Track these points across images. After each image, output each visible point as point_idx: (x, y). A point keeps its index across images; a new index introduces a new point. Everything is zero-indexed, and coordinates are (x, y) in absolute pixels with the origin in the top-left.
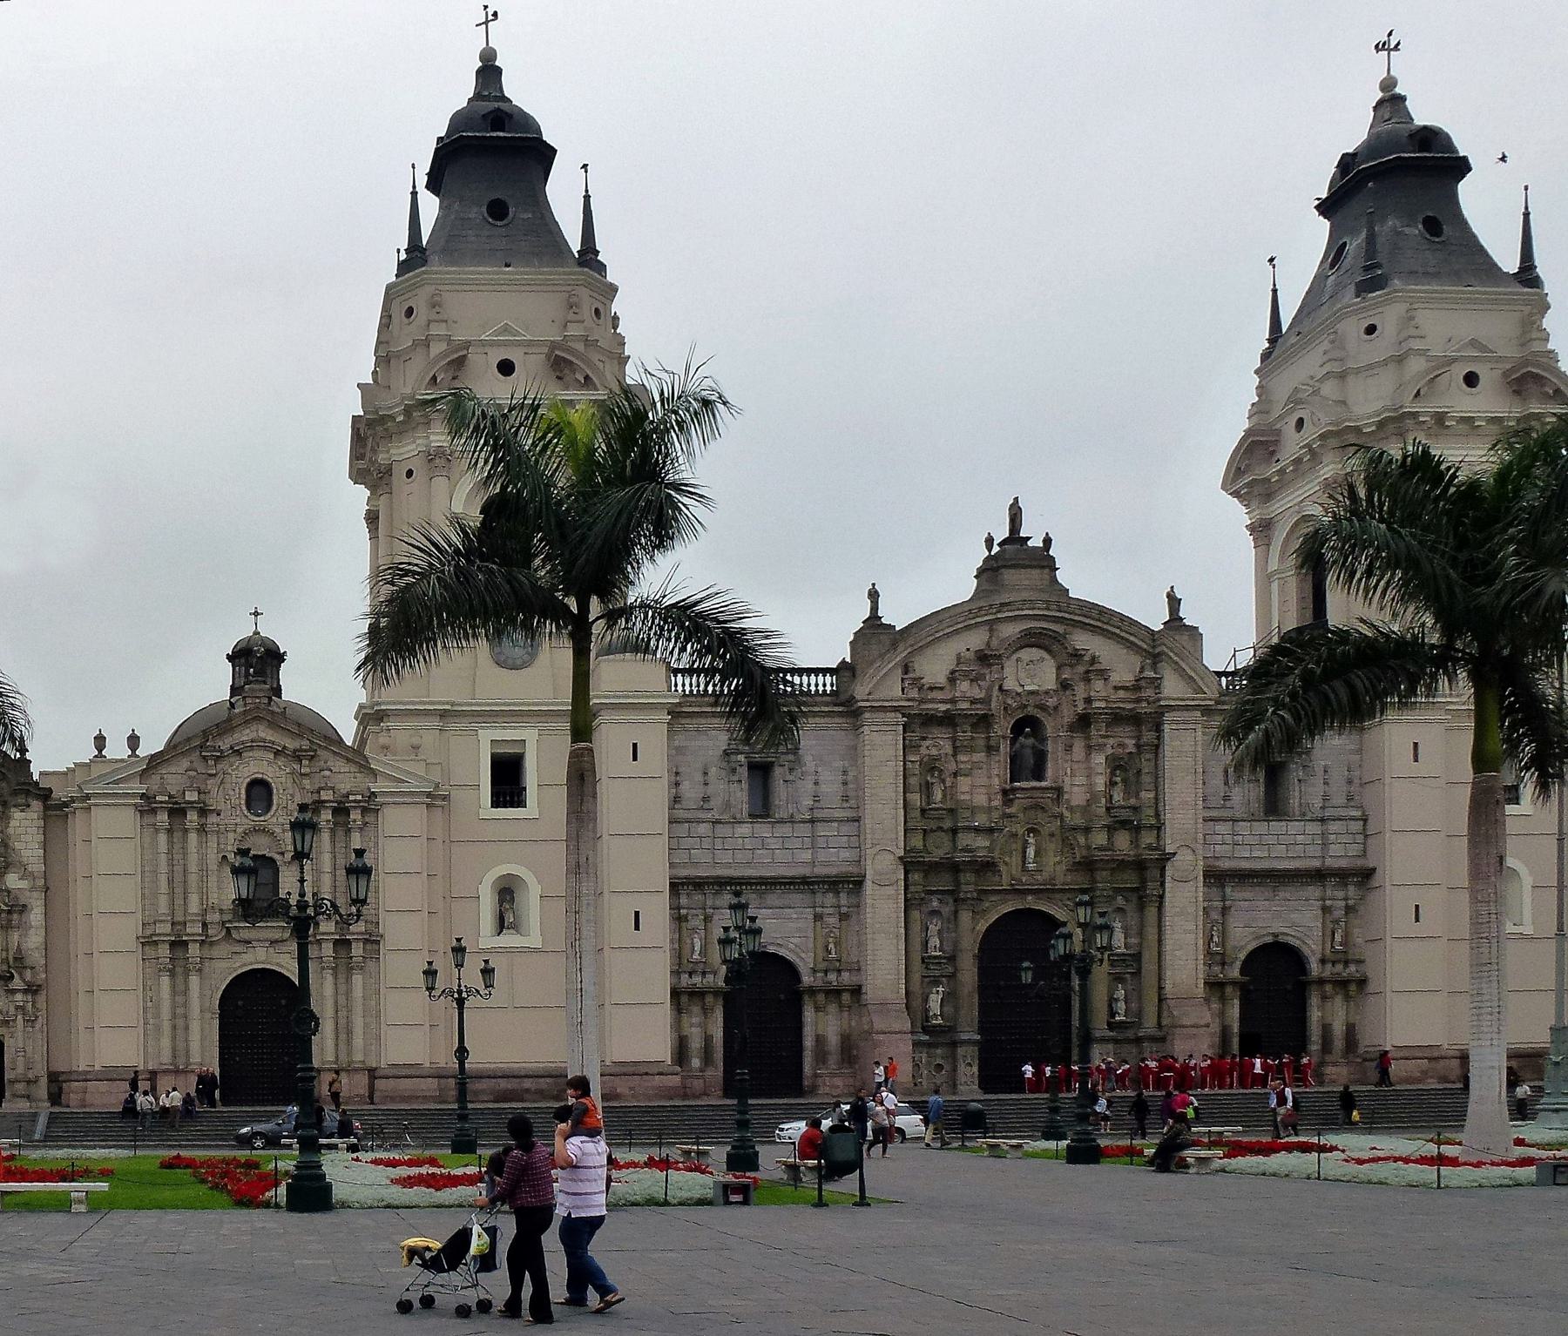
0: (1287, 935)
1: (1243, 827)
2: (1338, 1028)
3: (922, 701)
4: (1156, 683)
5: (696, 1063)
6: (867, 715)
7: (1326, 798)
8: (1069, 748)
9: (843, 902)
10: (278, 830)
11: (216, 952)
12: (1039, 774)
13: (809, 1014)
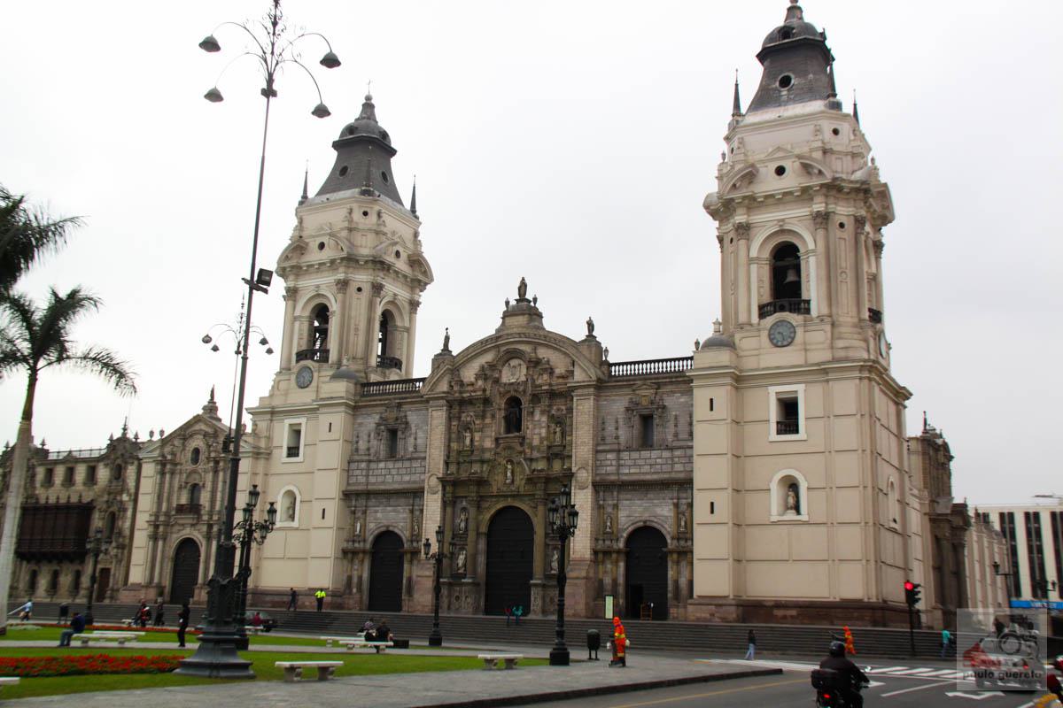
0: (653, 521)
1: (625, 455)
2: (683, 581)
3: (461, 393)
4: (572, 372)
5: (354, 590)
6: (431, 402)
7: (676, 435)
8: (532, 413)
10: (200, 471)
11: (176, 528)
12: (519, 429)
13: (406, 566)
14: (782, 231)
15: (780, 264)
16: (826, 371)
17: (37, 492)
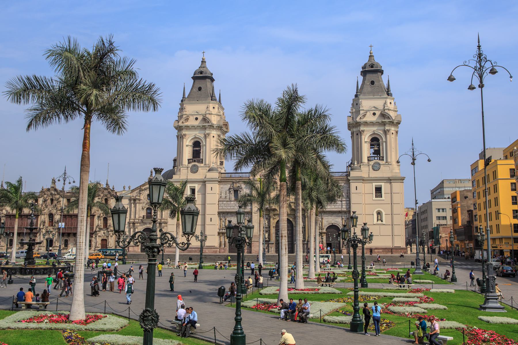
5: (223, 246)
9: (250, 216)
14: (374, 134)
16: (391, 180)
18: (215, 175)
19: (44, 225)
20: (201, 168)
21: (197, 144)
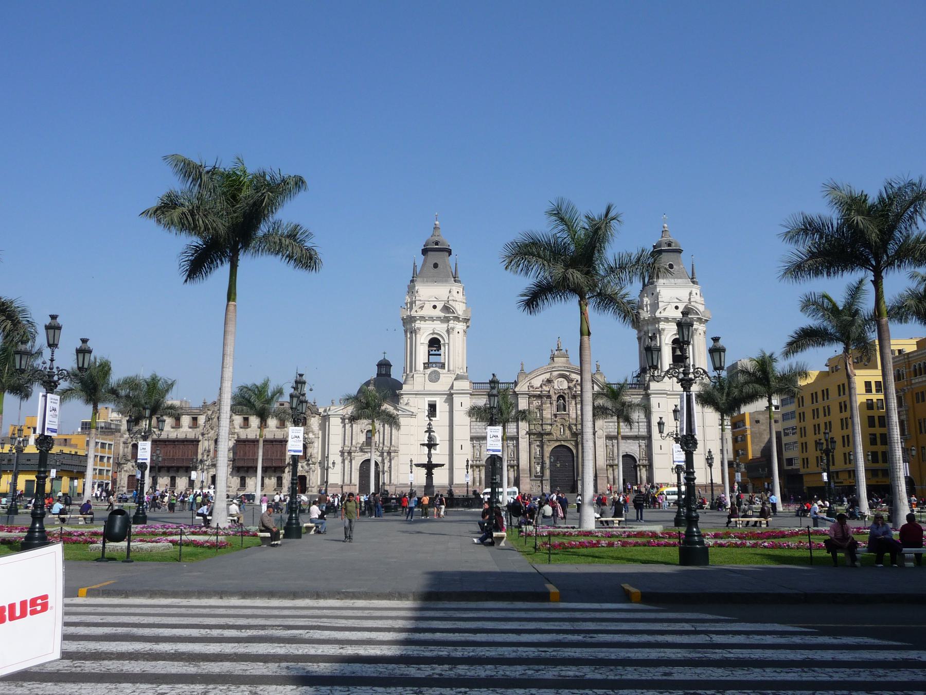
5: (478, 484)
15: (674, 346)
17: (236, 431)
18: (465, 385)
19: (208, 456)
20: (444, 375)
21: (435, 343)
